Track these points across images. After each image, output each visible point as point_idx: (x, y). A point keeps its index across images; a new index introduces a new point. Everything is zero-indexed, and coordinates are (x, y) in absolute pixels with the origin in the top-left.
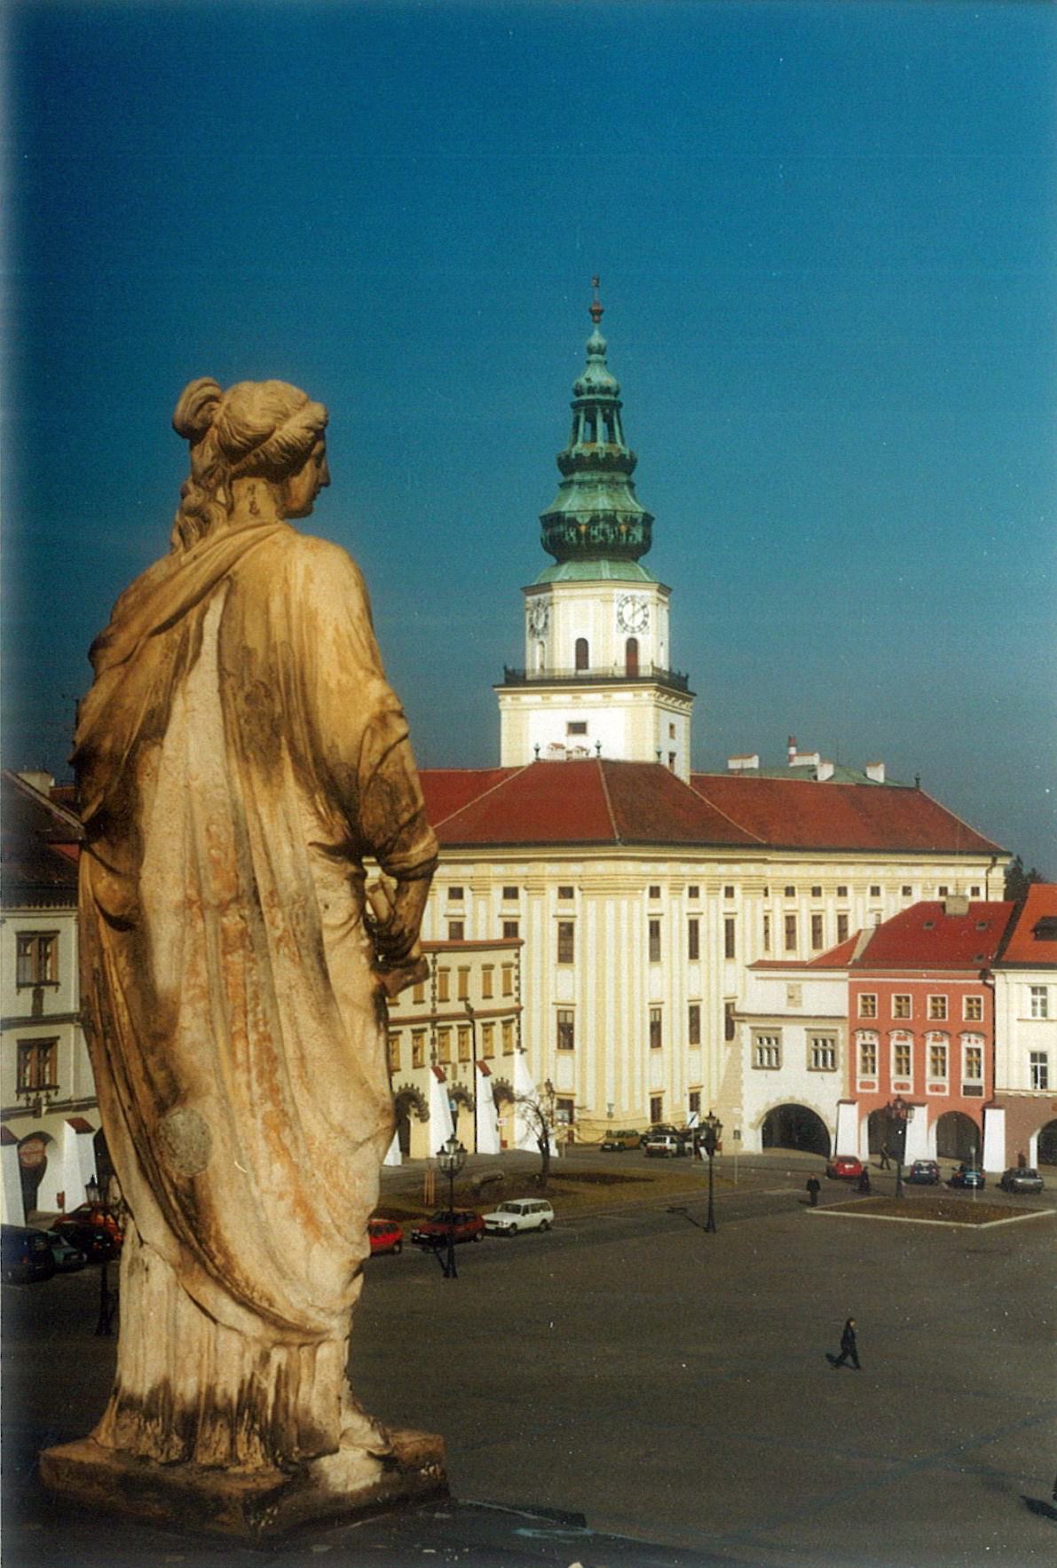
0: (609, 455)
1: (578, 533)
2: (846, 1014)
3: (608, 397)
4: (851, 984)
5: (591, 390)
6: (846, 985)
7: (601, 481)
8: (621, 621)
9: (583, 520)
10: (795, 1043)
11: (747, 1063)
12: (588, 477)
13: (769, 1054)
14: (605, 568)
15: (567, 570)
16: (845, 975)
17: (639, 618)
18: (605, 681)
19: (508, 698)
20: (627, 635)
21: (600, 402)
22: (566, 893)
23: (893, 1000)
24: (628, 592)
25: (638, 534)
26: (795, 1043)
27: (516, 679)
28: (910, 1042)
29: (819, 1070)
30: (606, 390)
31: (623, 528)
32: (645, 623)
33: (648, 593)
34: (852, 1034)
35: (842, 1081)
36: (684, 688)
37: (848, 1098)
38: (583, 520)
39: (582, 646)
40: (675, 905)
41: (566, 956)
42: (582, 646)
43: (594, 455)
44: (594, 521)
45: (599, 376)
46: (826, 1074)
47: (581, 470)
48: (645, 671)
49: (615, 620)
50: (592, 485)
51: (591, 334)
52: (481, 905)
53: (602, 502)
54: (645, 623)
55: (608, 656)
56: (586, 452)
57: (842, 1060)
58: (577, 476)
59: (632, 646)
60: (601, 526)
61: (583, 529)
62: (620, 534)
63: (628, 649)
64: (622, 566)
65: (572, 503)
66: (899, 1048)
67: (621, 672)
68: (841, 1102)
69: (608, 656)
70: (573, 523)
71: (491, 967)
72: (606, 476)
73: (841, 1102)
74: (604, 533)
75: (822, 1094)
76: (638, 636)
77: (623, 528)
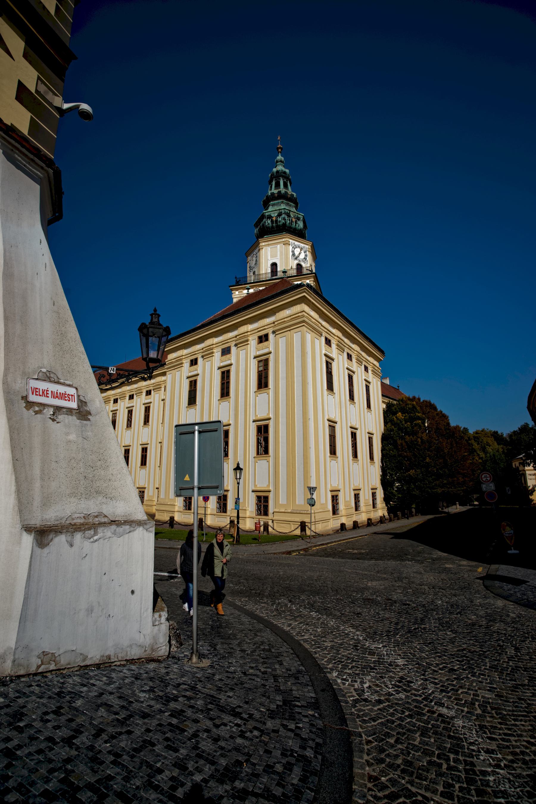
0: (286, 192)
1: (272, 221)
7: (282, 202)
8: (294, 255)
9: (274, 215)
17: (302, 256)
19: (237, 293)
20: (296, 262)
25: (301, 225)
31: (294, 220)
33: (307, 246)
38: (274, 215)
39: (274, 265)
40: (340, 357)
42: (274, 265)
43: (279, 192)
44: (280, 215)
45: (280, 168)
49: (291, 254)
56: (276, 192)
58: (271, 202)
59: (299, 266)
60: (283, 216)
61: (274, 219)
62: (292, 221)
67: (294, 273)
70: (270, 217)
74: (284, 219)
76: (303, 264)
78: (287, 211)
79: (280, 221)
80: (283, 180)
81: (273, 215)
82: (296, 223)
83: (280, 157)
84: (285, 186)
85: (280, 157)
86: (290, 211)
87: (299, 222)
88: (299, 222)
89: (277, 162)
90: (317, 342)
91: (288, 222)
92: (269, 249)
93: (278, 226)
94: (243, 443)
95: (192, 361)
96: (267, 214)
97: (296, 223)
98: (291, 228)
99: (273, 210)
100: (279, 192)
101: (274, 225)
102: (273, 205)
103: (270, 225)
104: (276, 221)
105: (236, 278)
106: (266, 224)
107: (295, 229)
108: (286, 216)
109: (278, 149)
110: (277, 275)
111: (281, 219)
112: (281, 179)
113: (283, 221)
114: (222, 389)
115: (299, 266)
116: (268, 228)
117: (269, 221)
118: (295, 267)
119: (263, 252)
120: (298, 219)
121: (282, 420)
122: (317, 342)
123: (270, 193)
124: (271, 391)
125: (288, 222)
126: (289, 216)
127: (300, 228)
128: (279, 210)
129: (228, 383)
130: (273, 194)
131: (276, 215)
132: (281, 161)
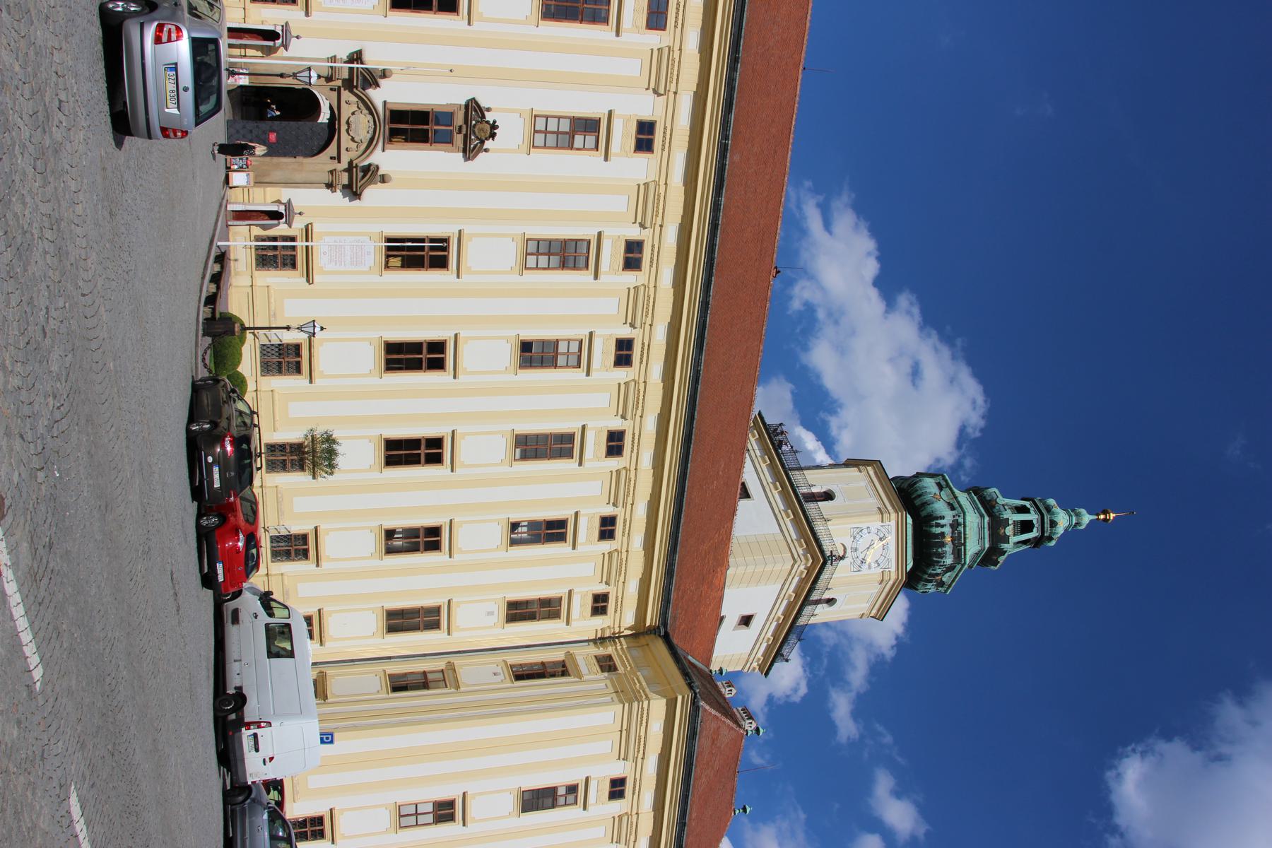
30: (1053, 524)
33: (893, 569)
39: (828, 496)
42: (828, 496)
51: (1090, 513)
83: (1087, 518)
85: (1087, 518)
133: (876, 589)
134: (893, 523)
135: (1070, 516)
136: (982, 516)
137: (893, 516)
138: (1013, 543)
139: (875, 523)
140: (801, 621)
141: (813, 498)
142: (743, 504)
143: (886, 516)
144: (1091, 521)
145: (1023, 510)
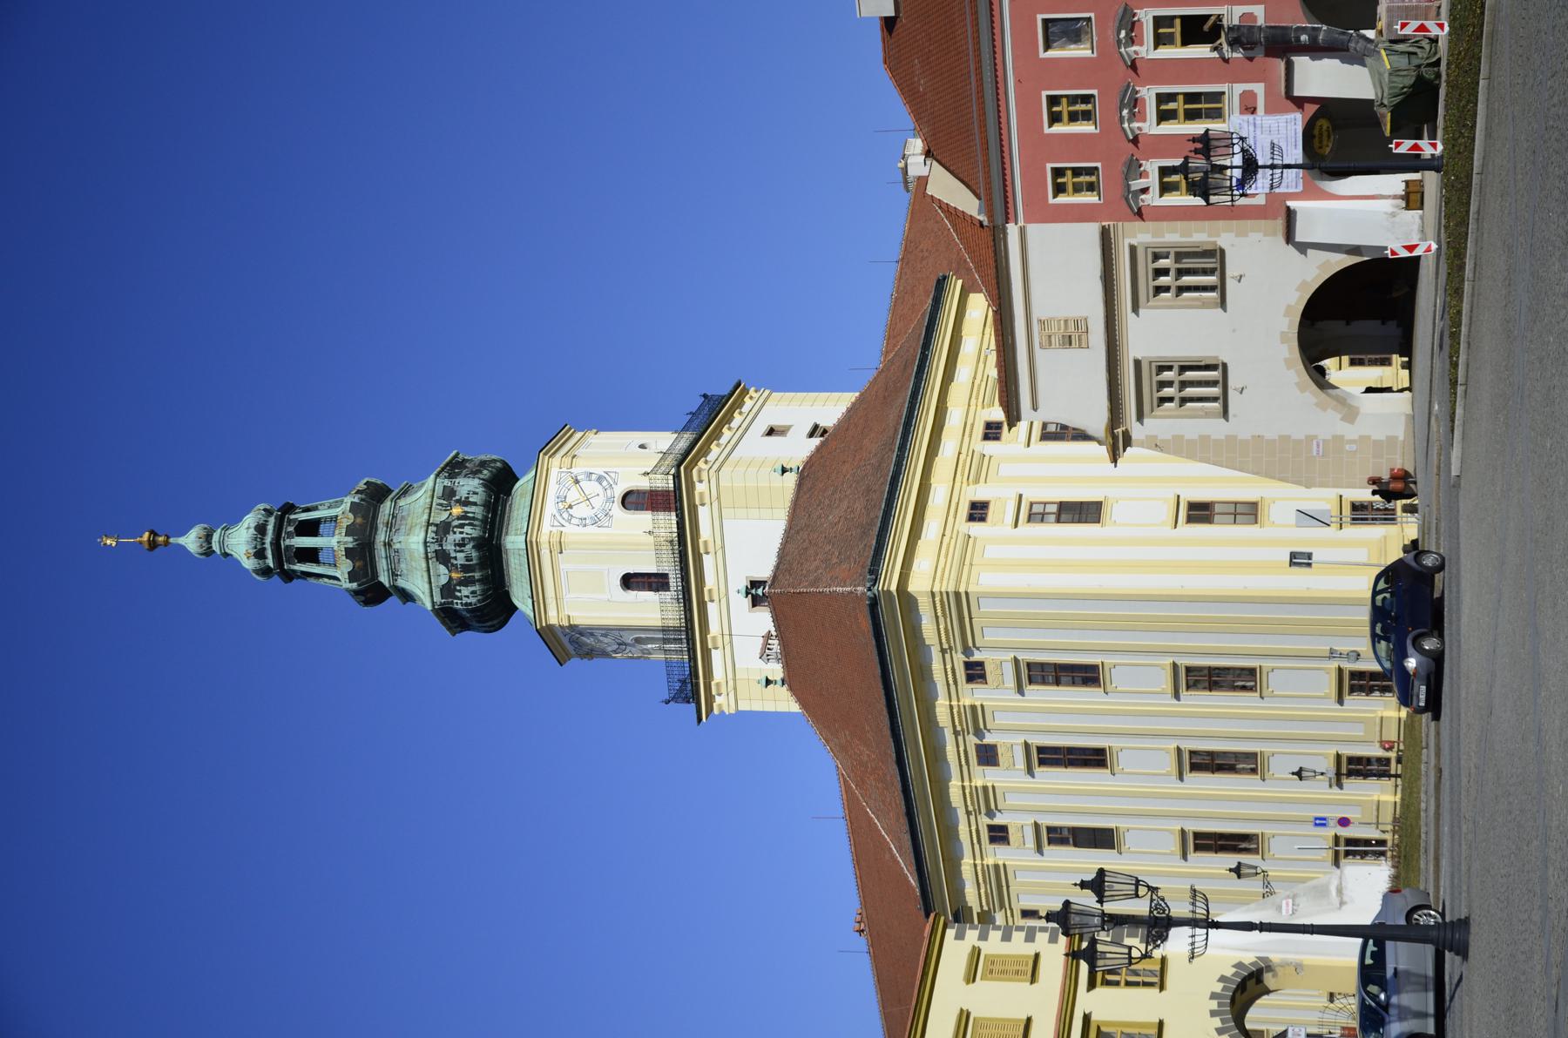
1: (466, 582)
2: (1092, 230)
3: (270, 528)
4: (1027, 220)
5: (260, 554)
6: (1032, 229)
9: (442, 574)
10: (1161, 331)
11: (1216, 428)
12: (382, 565)
13: (1200, 382)
14: (513, 542)
15: (520, 597)
16: (1012, 230)
17: (591, 487)
18: (685, 546)
20: (617, 508)
21: (276, 544)
22: (975, 672)
23: (1058, 129)
24: (550, 507)
25: (469, 486)
26: (1161, 331)
27: (689, 687)
28: (1148, 94)
29: (1221, 288)
30: (261, 529)
31: (457, 511)
32: (600, 479)
34: (1140, 214)
35: (1241, 234)
36: (722, 401)
37: (1280, 224)
38: (442, 574)
39: (629, 581)
41: (1087, 676)
42: (629, 581)
43: (349, 553)
44: (443, 557)
45: (239, 541)
46: (1231, 271)
47: (375, 574)
48: (664, 483)
50: (394, 557)
51: (182, 548)
52: (1012, 801)
53: (413, 541)
54: (600, 479)
55: (644, 539)
57: (1198, 235)
58: (384, 579)
59: (632, 500)
60: (449, 547)
62: (464, 517)
63: (638, 507)
64: (515, 514)
65: (421, 583)
66: (1163, 116)
68: (1289, 236)
69: (644, 539)
70: (448, 590)
71: (964, 1017)
72: (381, 537)
73: (1289, 236)
75: (1272, 283)
76: (619, 491)
77: (457, 511)
78: (431, 535)
79: (468, 559)
80: (290, 535)
81: (444, 580)
82: (466, 503)
83: (191, 541)
84: (311, 528)
85: (191, 541)
86: (429, 524)
87: (462, 493)
88: (462, 493)
89: (209, 552)
90: (992, 552)
91: (467, 529)
92: (569, 597)
93: (482, 565)
94: (1218, 719)
95: (993, 840)
96: (438, 598)
97: (465, 503)
98: (484, 521)
99: (420, 582)
100: (349, 553)
101: (477, 575)
102: (394, 574)
103: (477, 588)
104: (465, 568)
105: (667, 702)
106: (473, 600)
107: (487, 505)
108: (451, 537)
109: (153, 545)
110: (665, 576)
111: (460, 555)
112: (288, 542)
113: (469, 547)
114: (1086, 763)
115: (632, 500)
116: (484, 592)
117: (465, 591)
118: (645, 518)
119: (583, 616)
120: (449, 494)
121: (1181, 642)
122: (992, 552)
123: (346, 584)
124: (1109, 660)
125: (467, 529)
126: (444, 528)
127: (480, 490)
128: (427, 559)
129: (1071, 750)
130: (352, 576)
131: (442, 569)
132: (208, 537)
133: (580, 451)
134: (546, 527)
135: (222, 543)
136: (388, 545)
137: (544, 539)
138: (341, 509)
139: (571, 531)
140: (688, 437)
141: (655, 582)
142: (765, 571)
143: (555, 540)
144: (183, 533)
145: (311, 555)
